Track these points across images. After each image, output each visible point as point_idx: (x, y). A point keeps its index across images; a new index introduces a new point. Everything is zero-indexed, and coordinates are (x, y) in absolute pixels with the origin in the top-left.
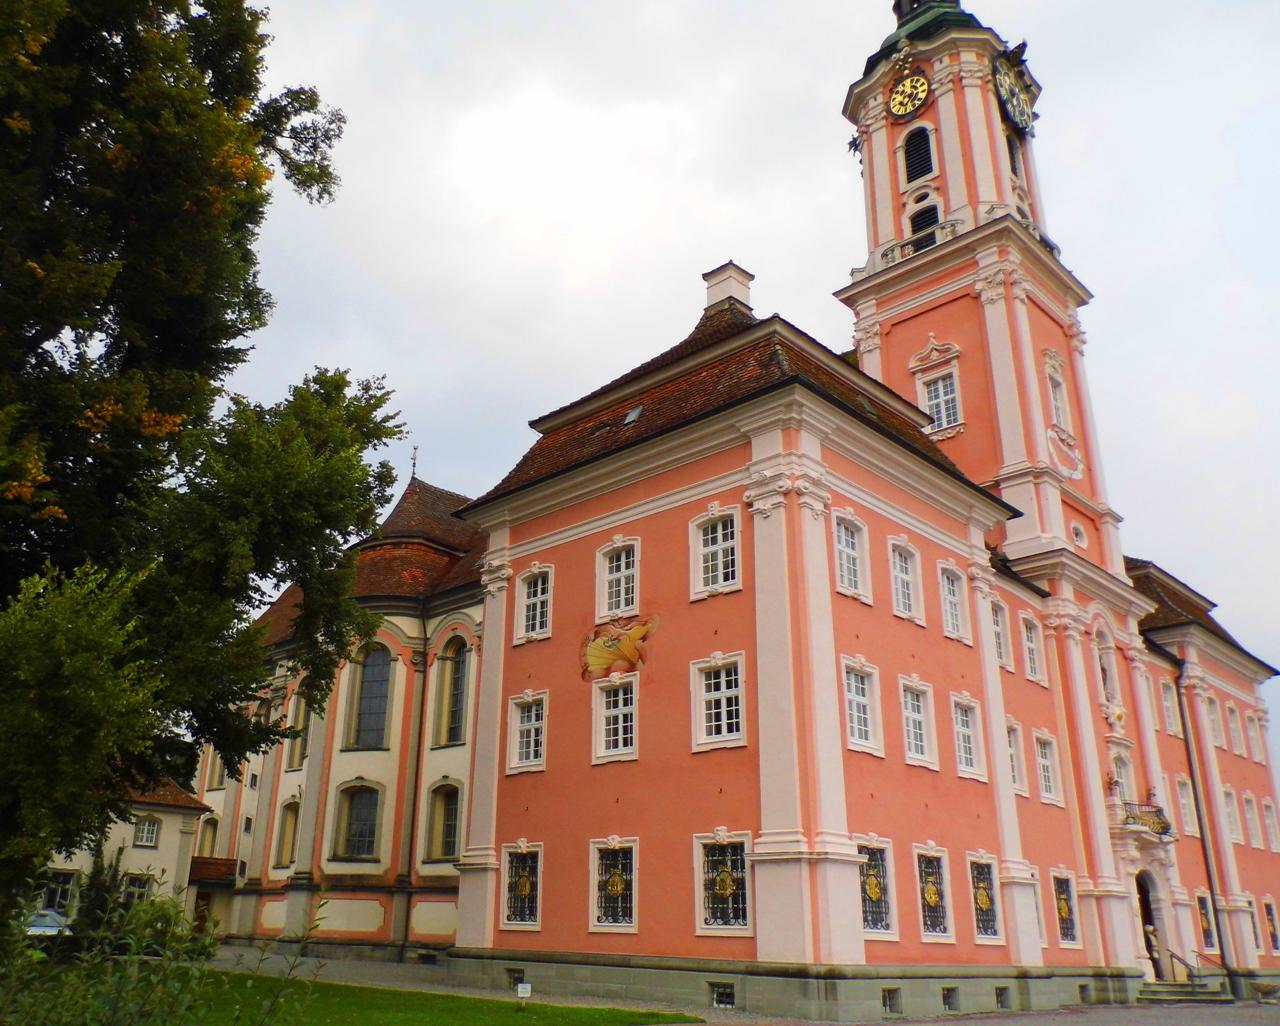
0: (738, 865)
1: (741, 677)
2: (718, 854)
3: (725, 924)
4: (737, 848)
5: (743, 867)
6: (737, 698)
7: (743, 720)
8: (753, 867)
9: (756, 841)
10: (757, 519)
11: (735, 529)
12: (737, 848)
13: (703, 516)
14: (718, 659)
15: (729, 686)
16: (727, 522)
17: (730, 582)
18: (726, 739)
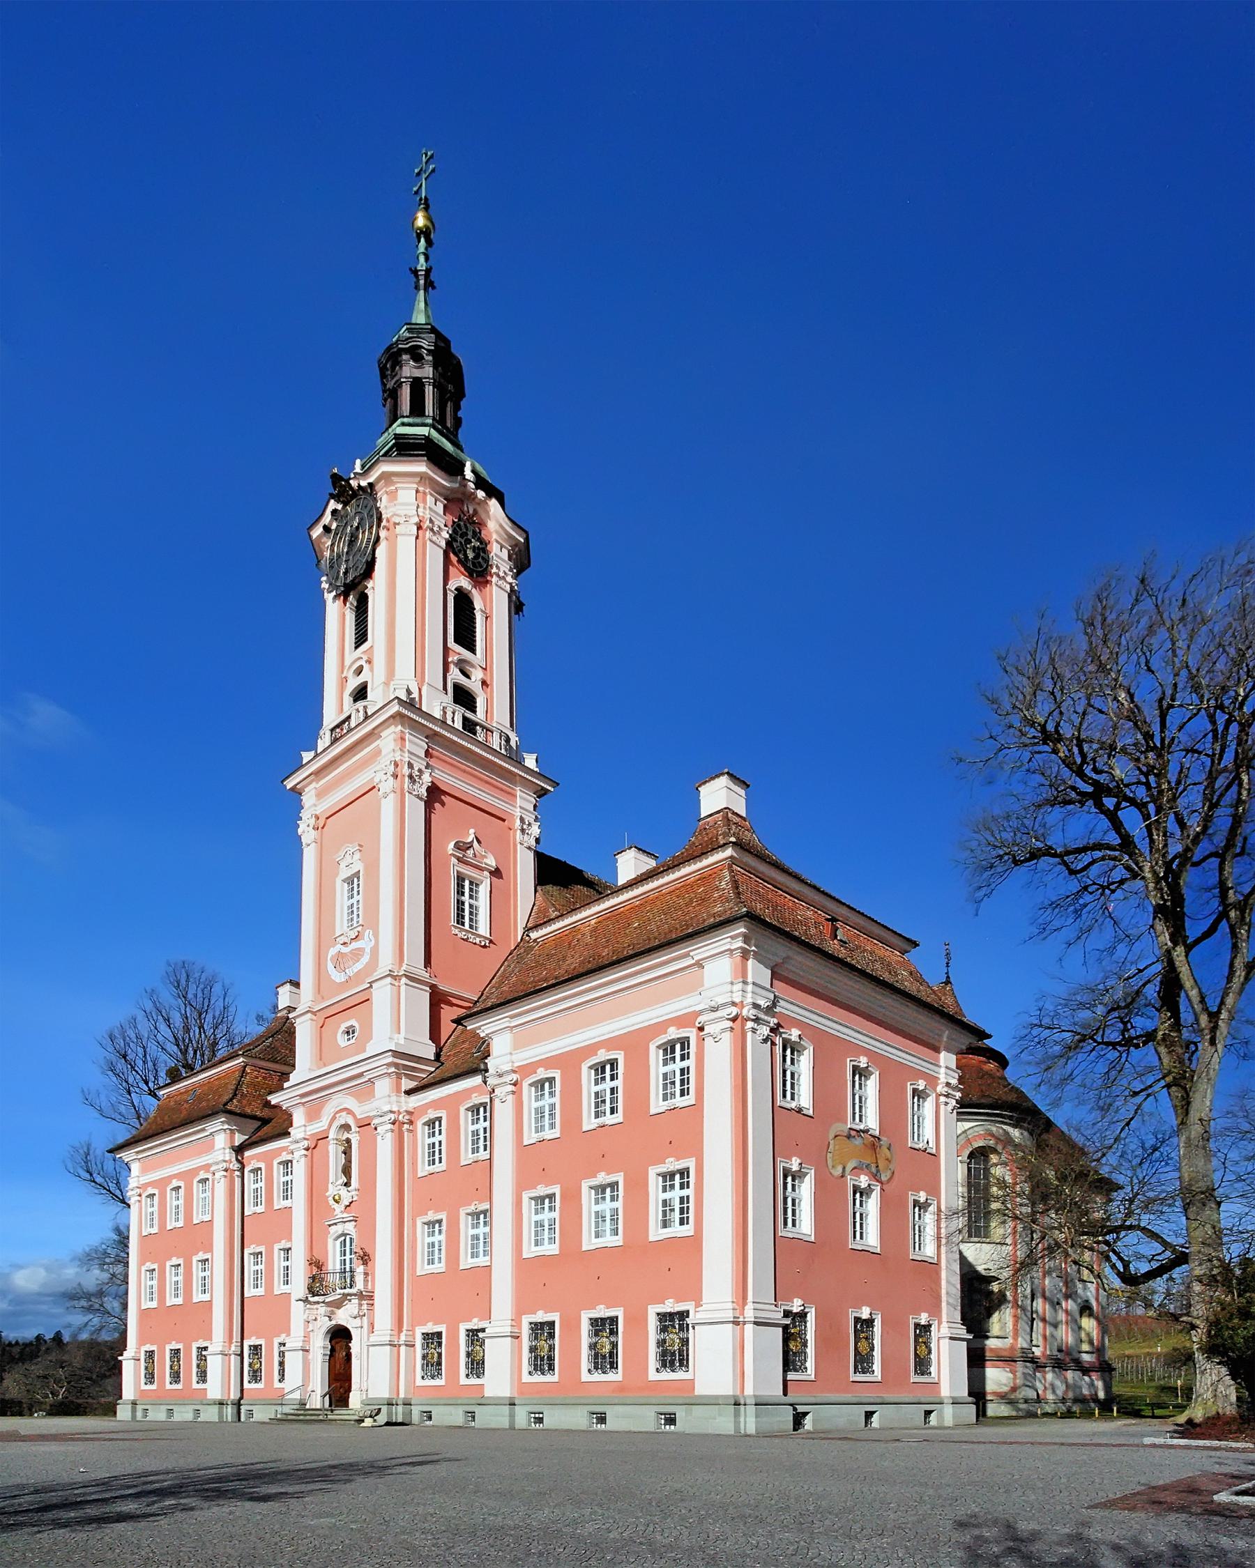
0: (684, 1328)
1: (692, 1179)
2: (667, 1320)
3: (673, 1371)
4: (683, 1315)
5: (688, 1330)
6: (688, 1197)
7: (691, 1215)
8: (694, 1329)
9: (697, 1309)
10: (709, 1042)
11: (690, 1050)
12: (683, 1315)
13: (662, 1039)
14: (672, 1164)
15: (682, 1187)
16: (684, 1042)
17: (686, 1097)
18: (677, 1230)
